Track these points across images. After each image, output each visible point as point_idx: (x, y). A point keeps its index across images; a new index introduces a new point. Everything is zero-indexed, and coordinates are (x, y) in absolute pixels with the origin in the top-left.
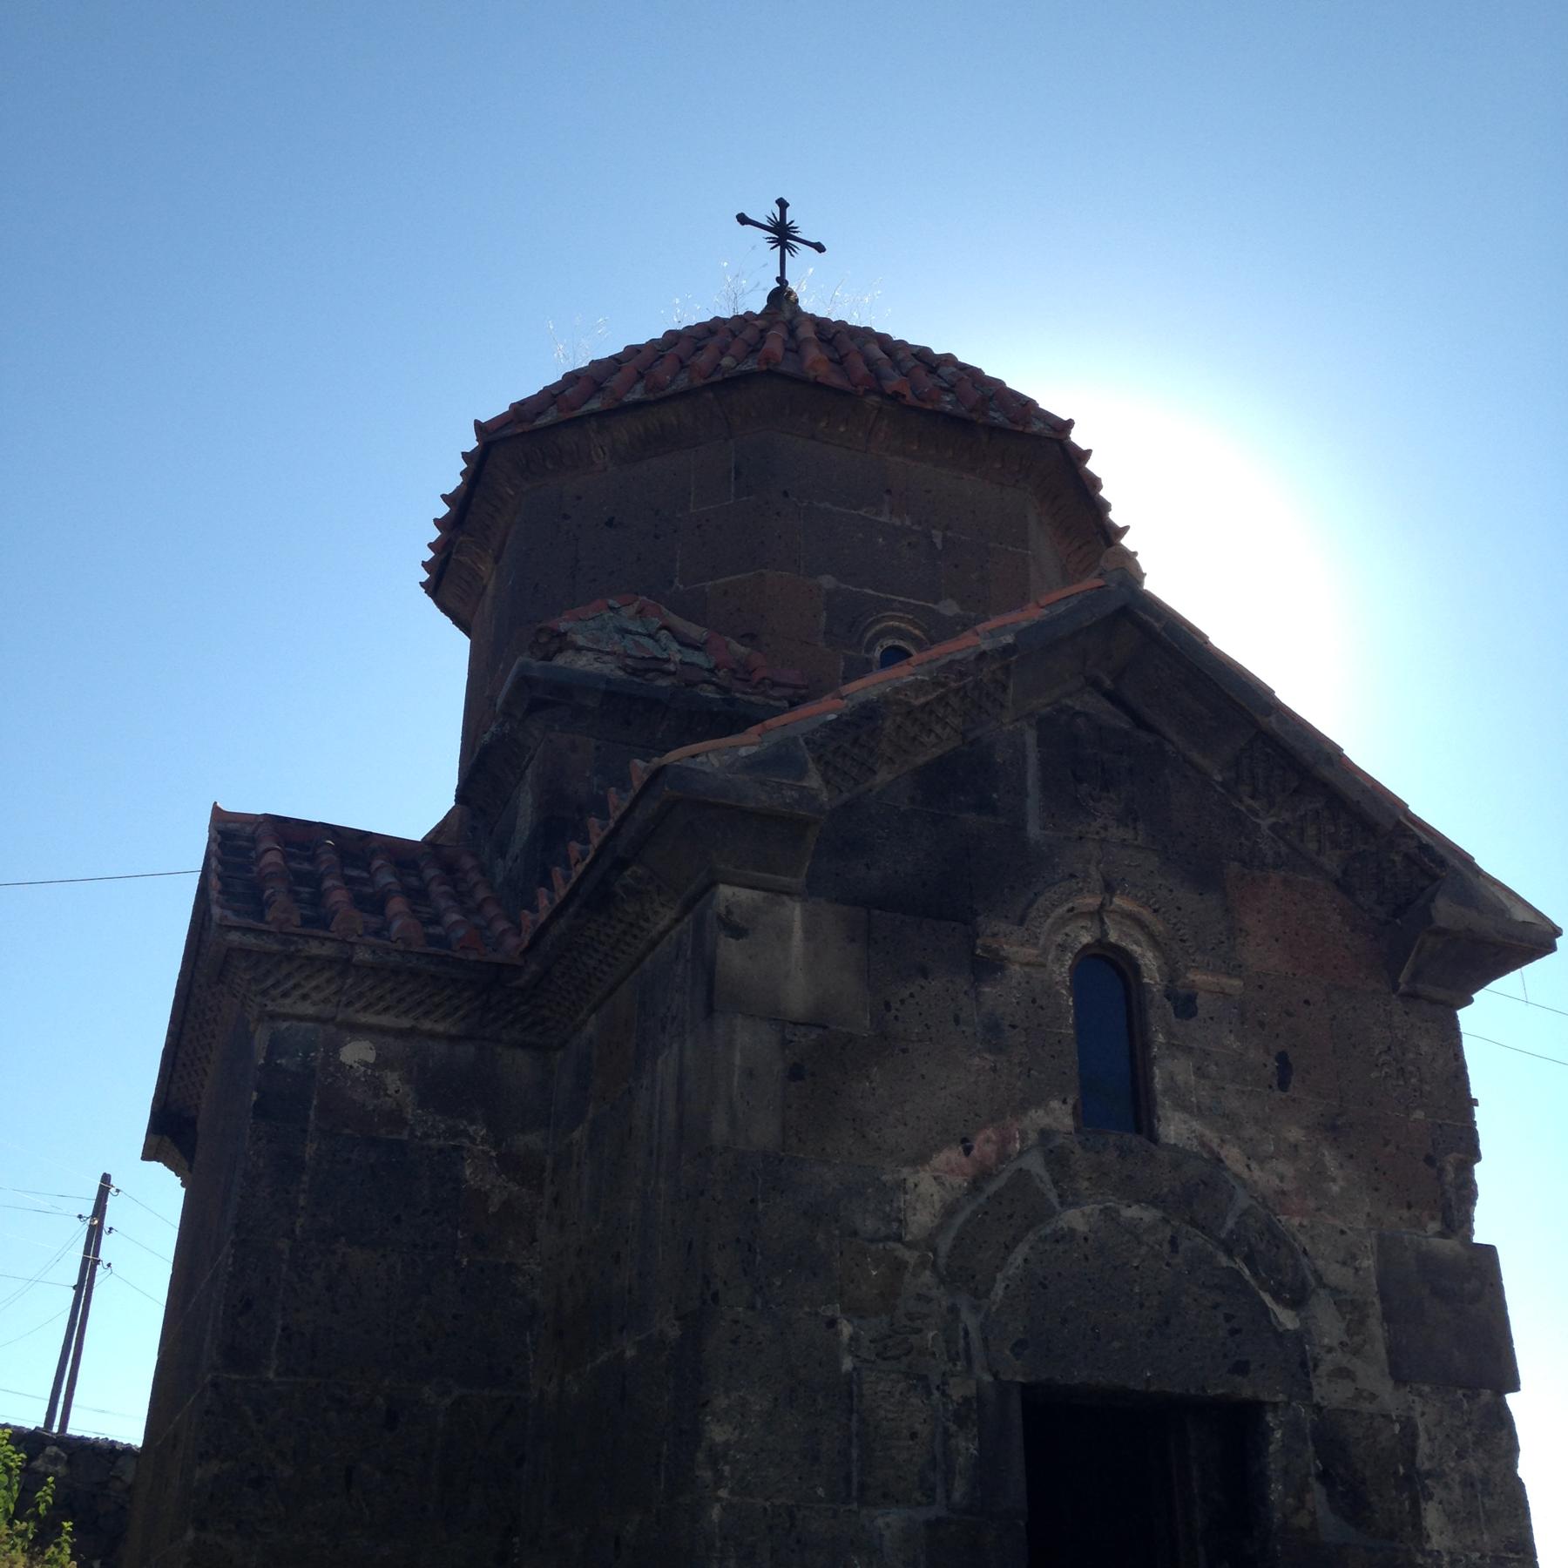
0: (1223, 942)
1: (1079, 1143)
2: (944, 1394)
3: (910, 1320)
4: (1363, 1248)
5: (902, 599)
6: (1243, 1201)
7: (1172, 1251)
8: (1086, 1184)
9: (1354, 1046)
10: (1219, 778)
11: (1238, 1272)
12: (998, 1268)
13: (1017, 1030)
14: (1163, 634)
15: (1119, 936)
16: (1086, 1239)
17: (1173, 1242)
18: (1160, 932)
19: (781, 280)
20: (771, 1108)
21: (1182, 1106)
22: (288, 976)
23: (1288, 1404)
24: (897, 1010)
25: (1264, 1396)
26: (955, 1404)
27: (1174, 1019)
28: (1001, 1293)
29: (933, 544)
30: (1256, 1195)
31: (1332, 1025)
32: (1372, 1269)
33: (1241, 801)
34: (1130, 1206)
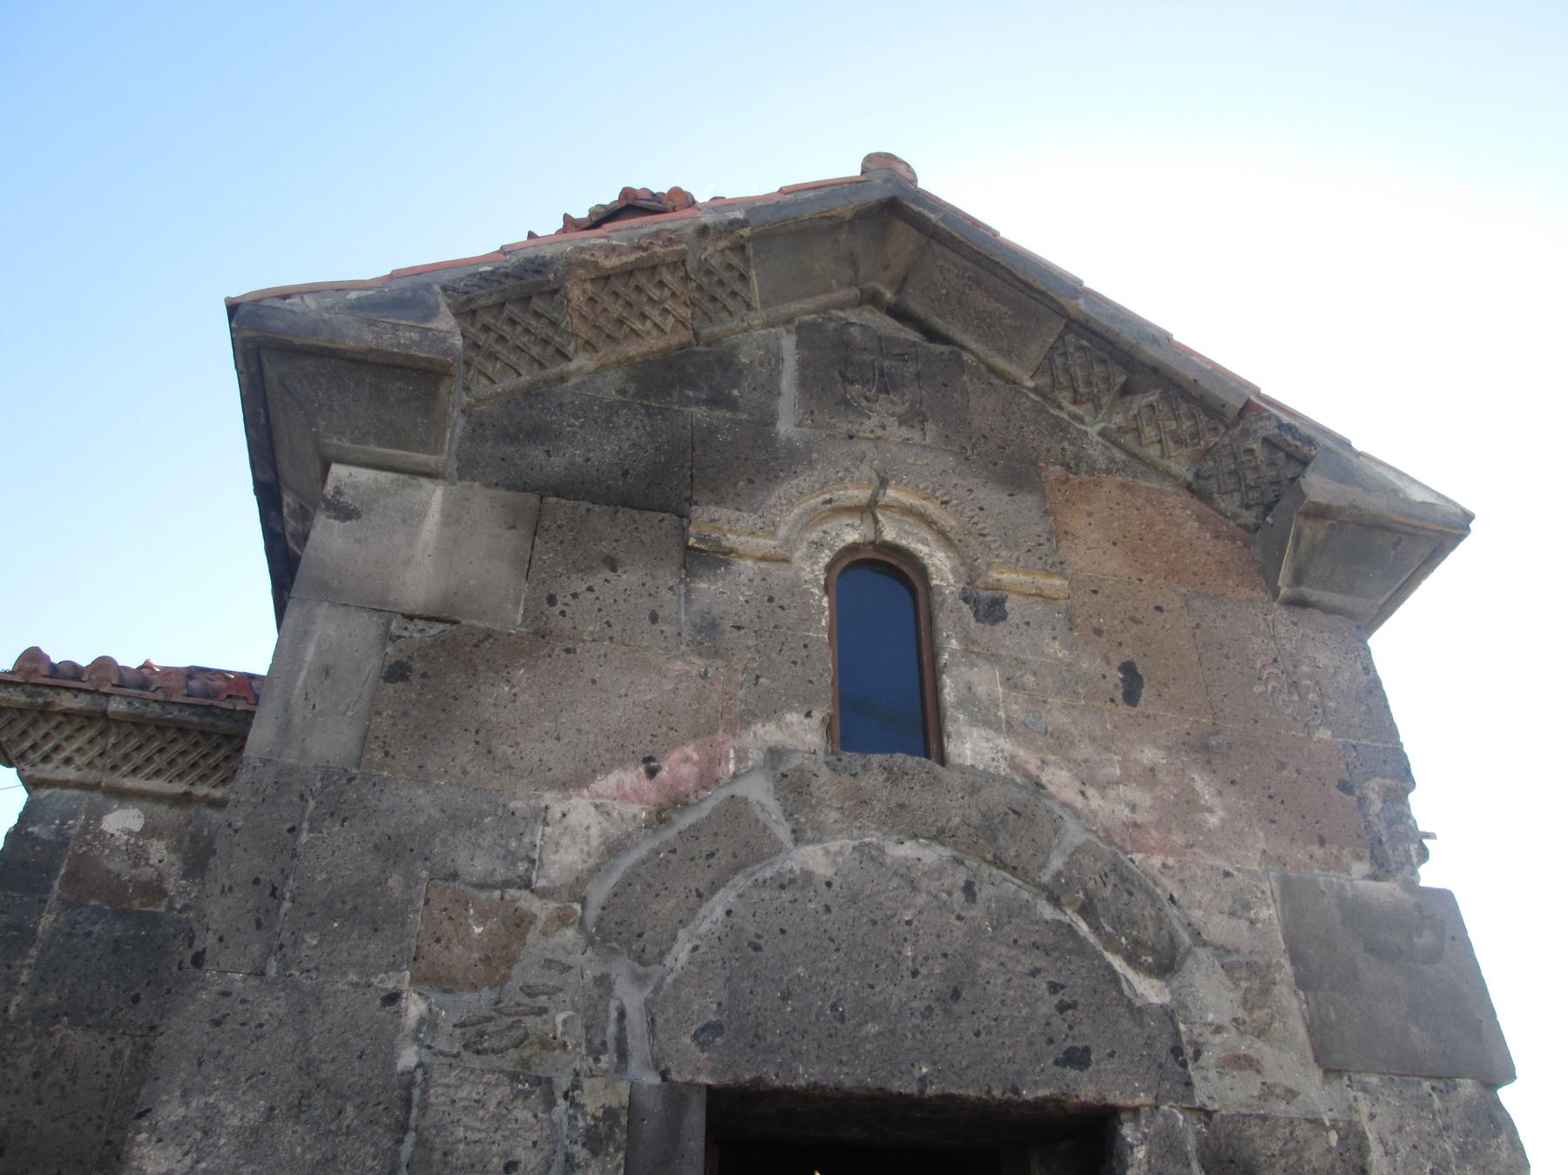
0: (1042, 545)
1: (827, 763)
2: (574, 1104)
3: (530, 995)
4: (1259, 895)
6: (1074, 834)
7: (967, 900)
8: (834, 815)
9: (1228, 658)
10: (1030, 384)
11: (1070, 926)
12: (682, 923)
13: (743, 631)
14: (941, 224)
15: (898, 534)
16: (829, 884)
17: (969, 890)
18: (952, 528)
20: (350, 714)
21: (983, 717)
22: (46, 736)
24: (566, 605)
25: (1116, 1098)
26: (589, 1118)
27: (973, 623)
28: (684, 957)
30: (1094, 828)
31: (1194, 635)
32: (1276, 921)
33: (1060, 407)
34: (902, 843)
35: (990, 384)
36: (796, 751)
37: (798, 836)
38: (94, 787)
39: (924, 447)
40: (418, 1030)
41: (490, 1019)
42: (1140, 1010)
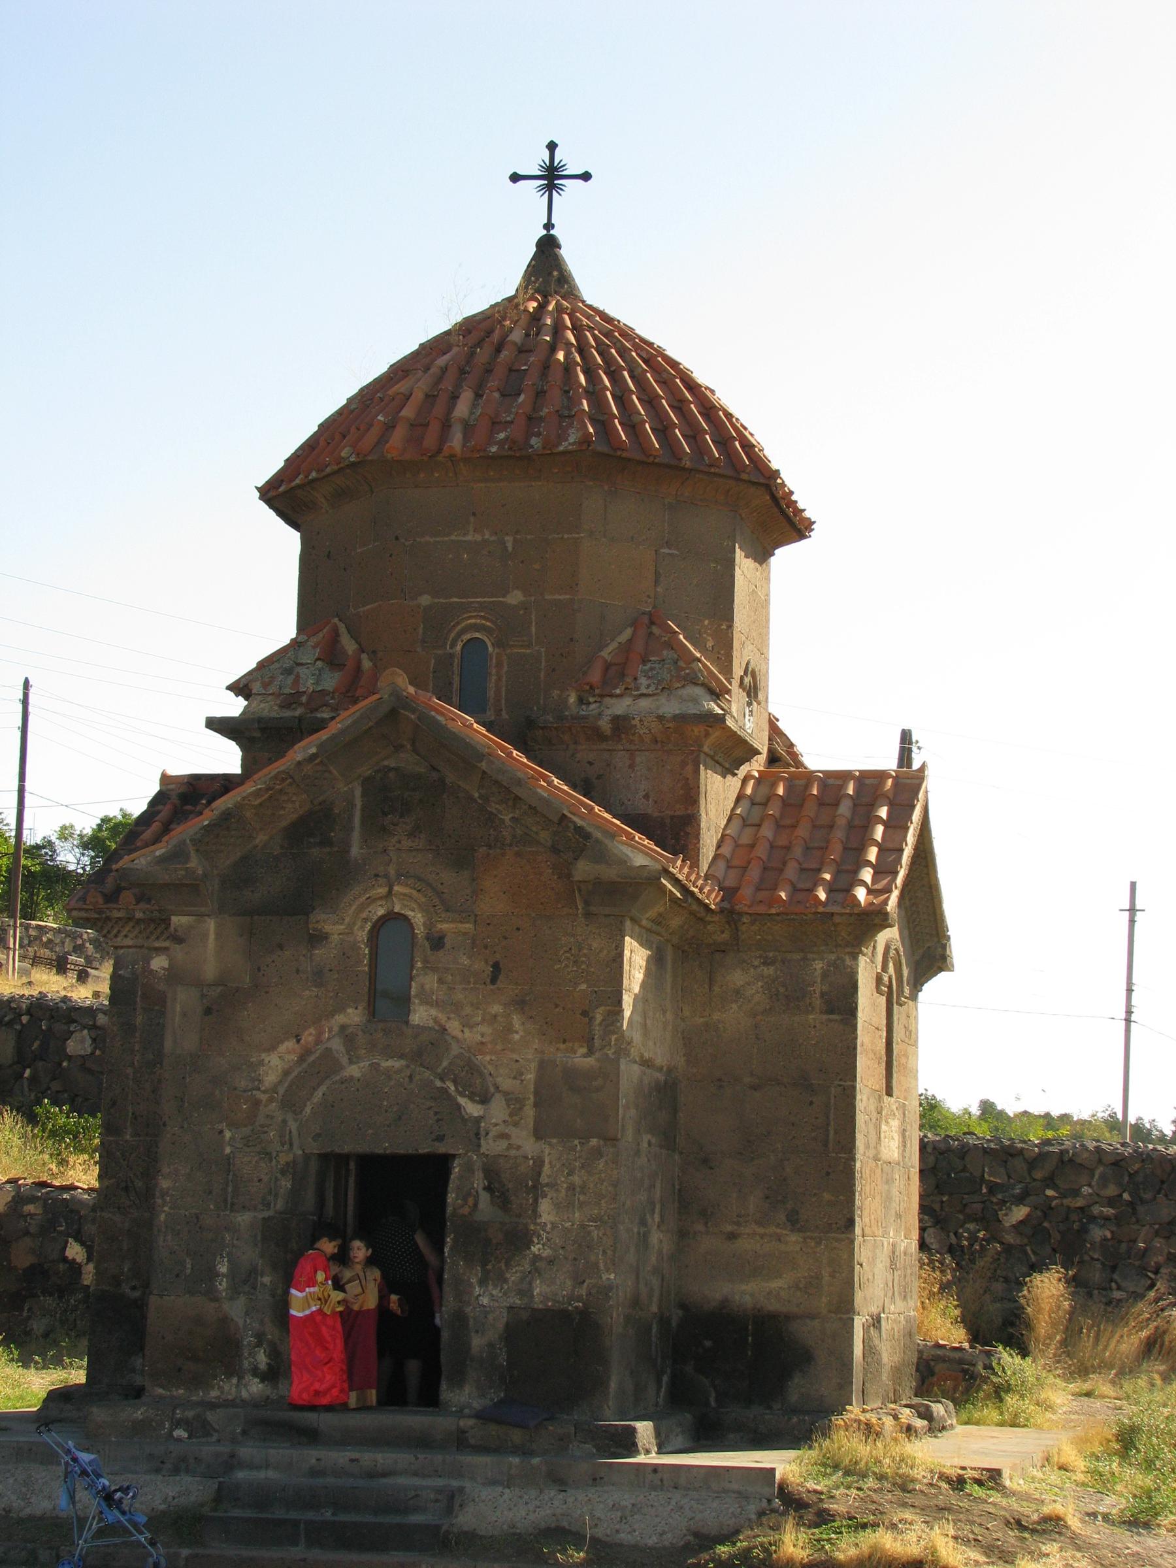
2: (278, 1162)
5: (478, 600)
6: (455, 1050)
8: (364, 1051)
9: (546, 951)
10: (476, 795)
12: (308, 1100)
15: (402, 909)
17: (411, 1077)
19: (549, 226)
21: (426, 1001)
23: (466, 1154)
25: (452, 1152)
27: (429, 952)
28: (309, 1111)
29: (506, 548)
35: (458, 797)
36: (348, 1026)
37: (351, 1062)
38: (142, 947)
39: (418, 850)
40: (230, 1141)
41: (250, 1136)
42: (466, 1120)
